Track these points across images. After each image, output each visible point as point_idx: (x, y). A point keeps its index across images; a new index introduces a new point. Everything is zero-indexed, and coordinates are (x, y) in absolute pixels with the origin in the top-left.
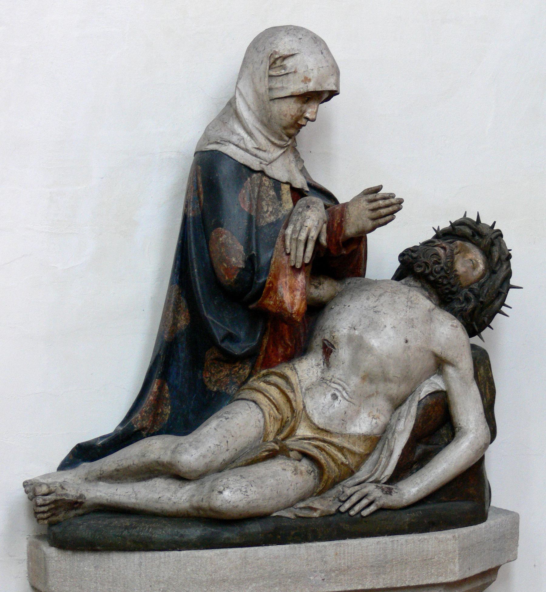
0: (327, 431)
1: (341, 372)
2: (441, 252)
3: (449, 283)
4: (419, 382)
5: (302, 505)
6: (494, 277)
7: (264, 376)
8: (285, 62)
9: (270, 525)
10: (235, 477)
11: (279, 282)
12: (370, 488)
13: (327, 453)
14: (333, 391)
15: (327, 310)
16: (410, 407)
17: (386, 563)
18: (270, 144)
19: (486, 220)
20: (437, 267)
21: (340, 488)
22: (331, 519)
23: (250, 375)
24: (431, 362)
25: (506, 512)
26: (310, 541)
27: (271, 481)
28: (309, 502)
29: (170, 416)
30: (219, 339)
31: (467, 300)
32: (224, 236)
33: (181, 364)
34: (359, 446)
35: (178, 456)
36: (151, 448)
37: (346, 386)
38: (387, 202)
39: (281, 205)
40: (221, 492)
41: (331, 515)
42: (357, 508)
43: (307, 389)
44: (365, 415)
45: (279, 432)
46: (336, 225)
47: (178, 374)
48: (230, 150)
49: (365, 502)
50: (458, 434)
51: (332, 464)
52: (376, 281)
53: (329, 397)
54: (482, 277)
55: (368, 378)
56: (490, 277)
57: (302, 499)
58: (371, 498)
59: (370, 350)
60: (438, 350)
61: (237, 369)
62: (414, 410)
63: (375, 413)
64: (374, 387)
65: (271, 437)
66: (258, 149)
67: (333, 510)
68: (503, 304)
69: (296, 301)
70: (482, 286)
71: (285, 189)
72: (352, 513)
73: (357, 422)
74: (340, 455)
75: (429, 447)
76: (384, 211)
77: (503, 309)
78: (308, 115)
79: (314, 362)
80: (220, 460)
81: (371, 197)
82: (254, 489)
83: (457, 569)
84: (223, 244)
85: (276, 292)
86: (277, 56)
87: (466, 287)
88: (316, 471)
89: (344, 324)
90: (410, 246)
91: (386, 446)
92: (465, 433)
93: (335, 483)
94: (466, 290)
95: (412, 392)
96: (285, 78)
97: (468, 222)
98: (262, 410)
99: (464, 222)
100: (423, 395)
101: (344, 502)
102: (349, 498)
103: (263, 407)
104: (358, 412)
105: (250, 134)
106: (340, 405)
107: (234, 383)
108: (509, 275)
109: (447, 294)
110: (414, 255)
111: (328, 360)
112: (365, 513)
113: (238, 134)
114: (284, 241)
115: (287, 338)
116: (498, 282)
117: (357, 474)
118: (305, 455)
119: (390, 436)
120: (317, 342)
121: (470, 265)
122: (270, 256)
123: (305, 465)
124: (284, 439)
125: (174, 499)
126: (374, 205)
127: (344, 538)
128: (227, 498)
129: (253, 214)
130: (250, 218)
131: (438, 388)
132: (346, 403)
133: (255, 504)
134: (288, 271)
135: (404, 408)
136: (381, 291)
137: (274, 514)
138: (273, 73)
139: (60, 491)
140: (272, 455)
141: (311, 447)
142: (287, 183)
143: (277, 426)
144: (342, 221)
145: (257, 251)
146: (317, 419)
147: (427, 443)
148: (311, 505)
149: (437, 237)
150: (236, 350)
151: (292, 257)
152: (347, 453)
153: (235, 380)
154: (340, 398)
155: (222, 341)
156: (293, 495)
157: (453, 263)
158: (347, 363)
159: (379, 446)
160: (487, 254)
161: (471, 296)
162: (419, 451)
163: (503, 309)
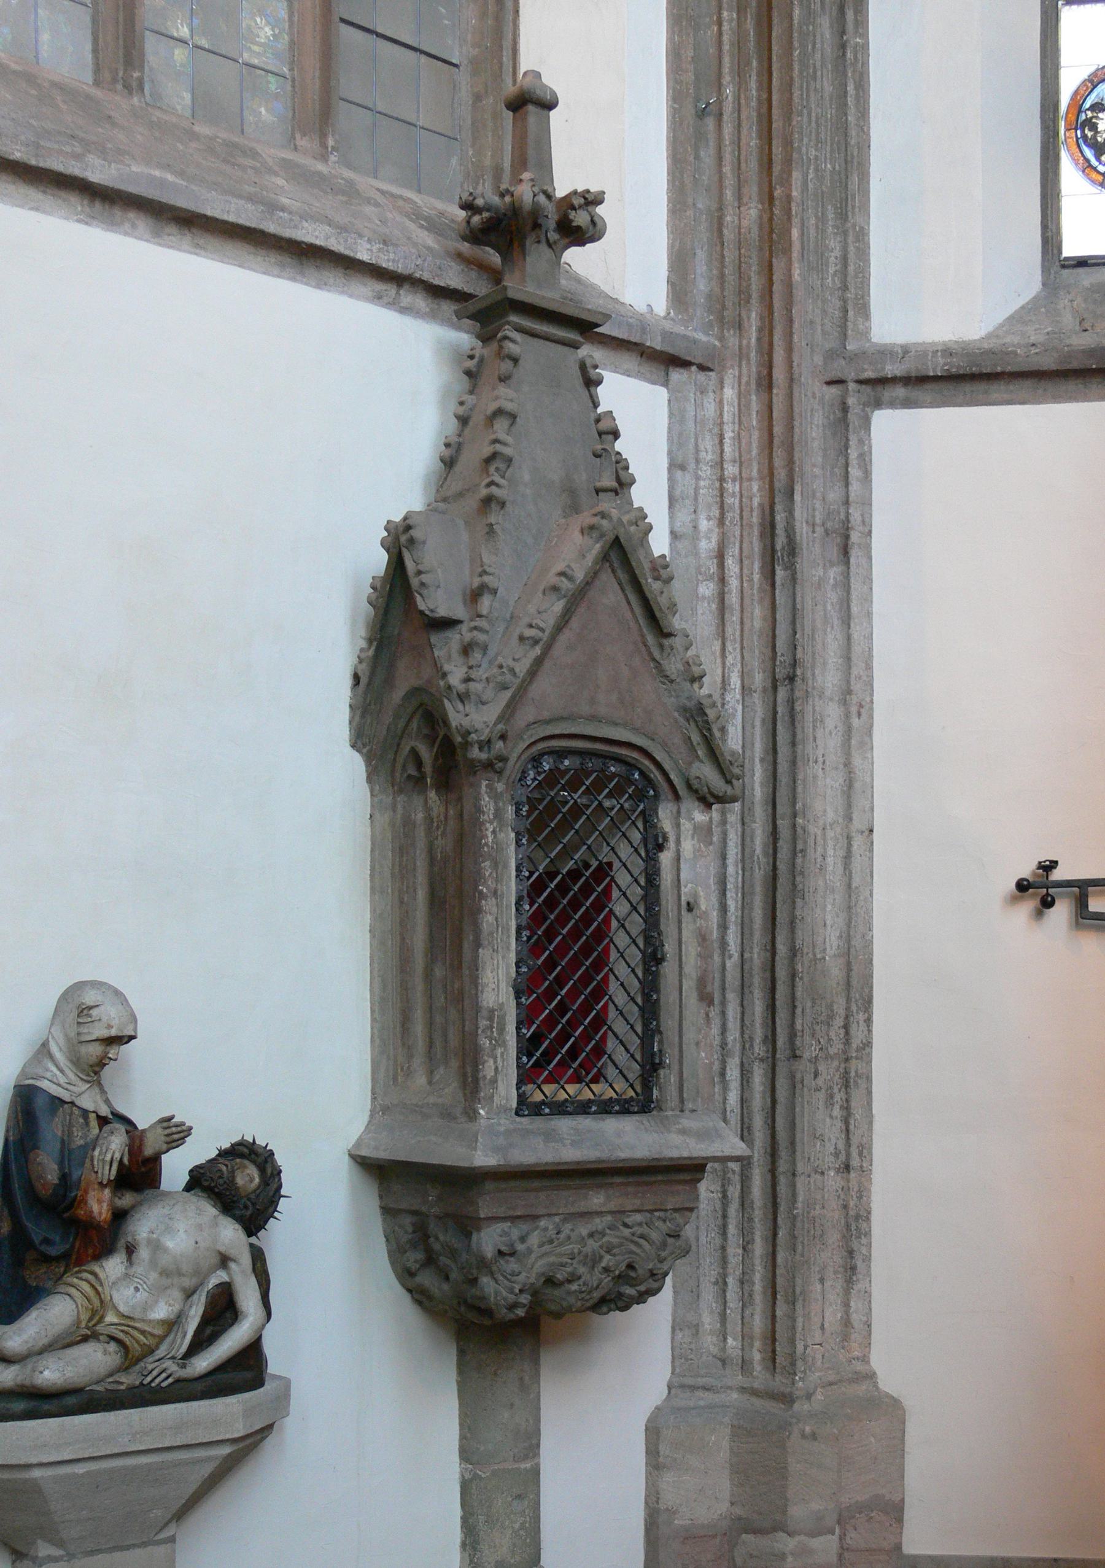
1: (142, 1268)
2: (224, 1168)
3: (231, 1194)
5: (110, 1380)
7: (77, 1272)
12: (168, 1364)
13: (132, 1337)
14: (135, 1285)
15: (128, 1216)
16: (200, 1296)
19: (261, 1142)
20: (221, 1181)
21: (142, 1364)
22: (135, 1390)
24: (216, 1260)
26: (118, 1410)
28: (116, 1378)
31: (246, 1207)
41: (135, 1388)
42: (157, 1381)
44: (163, 1304)
45: (90, 1319)
49: (164, 1375)
51: (136, 1345)
52: (170, 1193)
53: (132, 1289)
54: (258, 1188)
55: (165, 1273)
57: (111, 1375)
58: (169, 1372)
59: (166, 1250)
60: (223, 1249)
62: (203, 1299)
63: (172, 1302)
64: (169, 1281)
65: (83, 1325)
67: (137, 1383)
68: (275, 1210)
70: (258, 1196)
72: (153, 1385)
74: (142, 1337)
77: (276, 1214)
79: (119, 1261)
88: (123, 1351)
90: (198, 1163)
91: (180, 1329)
93: (139, 1360)
95: (202, 1284)
97: (245, 1143)
100: (210, 1286)
101: (146, 1376)
102: (151, 1372)
104: (157, 1302)
106: (142, 1296)
108: (280, 1186)
110: (202, 1171)
112: (164, 1384)
115: (95, 1241)
116: (271, 1193)
119: (184, 1320)
120: (121, 1244)
121: (247, 1179)
123: (113, 1347)
124: (95, 1325)
127: (147, 1406)
131: (223, 1280)
132: (147, 1294)
135: (196, 1297)
136: (175, 1201)
141: (117, 1332)
143: (88, 1314)
146: (122, 1308)
149: (218, 1155)
156: (103, 1371)
157: (234, 1177)
158: (147, 1261)
160: (262, 1169)
161: (249, 1203)
163: (276, 1214)
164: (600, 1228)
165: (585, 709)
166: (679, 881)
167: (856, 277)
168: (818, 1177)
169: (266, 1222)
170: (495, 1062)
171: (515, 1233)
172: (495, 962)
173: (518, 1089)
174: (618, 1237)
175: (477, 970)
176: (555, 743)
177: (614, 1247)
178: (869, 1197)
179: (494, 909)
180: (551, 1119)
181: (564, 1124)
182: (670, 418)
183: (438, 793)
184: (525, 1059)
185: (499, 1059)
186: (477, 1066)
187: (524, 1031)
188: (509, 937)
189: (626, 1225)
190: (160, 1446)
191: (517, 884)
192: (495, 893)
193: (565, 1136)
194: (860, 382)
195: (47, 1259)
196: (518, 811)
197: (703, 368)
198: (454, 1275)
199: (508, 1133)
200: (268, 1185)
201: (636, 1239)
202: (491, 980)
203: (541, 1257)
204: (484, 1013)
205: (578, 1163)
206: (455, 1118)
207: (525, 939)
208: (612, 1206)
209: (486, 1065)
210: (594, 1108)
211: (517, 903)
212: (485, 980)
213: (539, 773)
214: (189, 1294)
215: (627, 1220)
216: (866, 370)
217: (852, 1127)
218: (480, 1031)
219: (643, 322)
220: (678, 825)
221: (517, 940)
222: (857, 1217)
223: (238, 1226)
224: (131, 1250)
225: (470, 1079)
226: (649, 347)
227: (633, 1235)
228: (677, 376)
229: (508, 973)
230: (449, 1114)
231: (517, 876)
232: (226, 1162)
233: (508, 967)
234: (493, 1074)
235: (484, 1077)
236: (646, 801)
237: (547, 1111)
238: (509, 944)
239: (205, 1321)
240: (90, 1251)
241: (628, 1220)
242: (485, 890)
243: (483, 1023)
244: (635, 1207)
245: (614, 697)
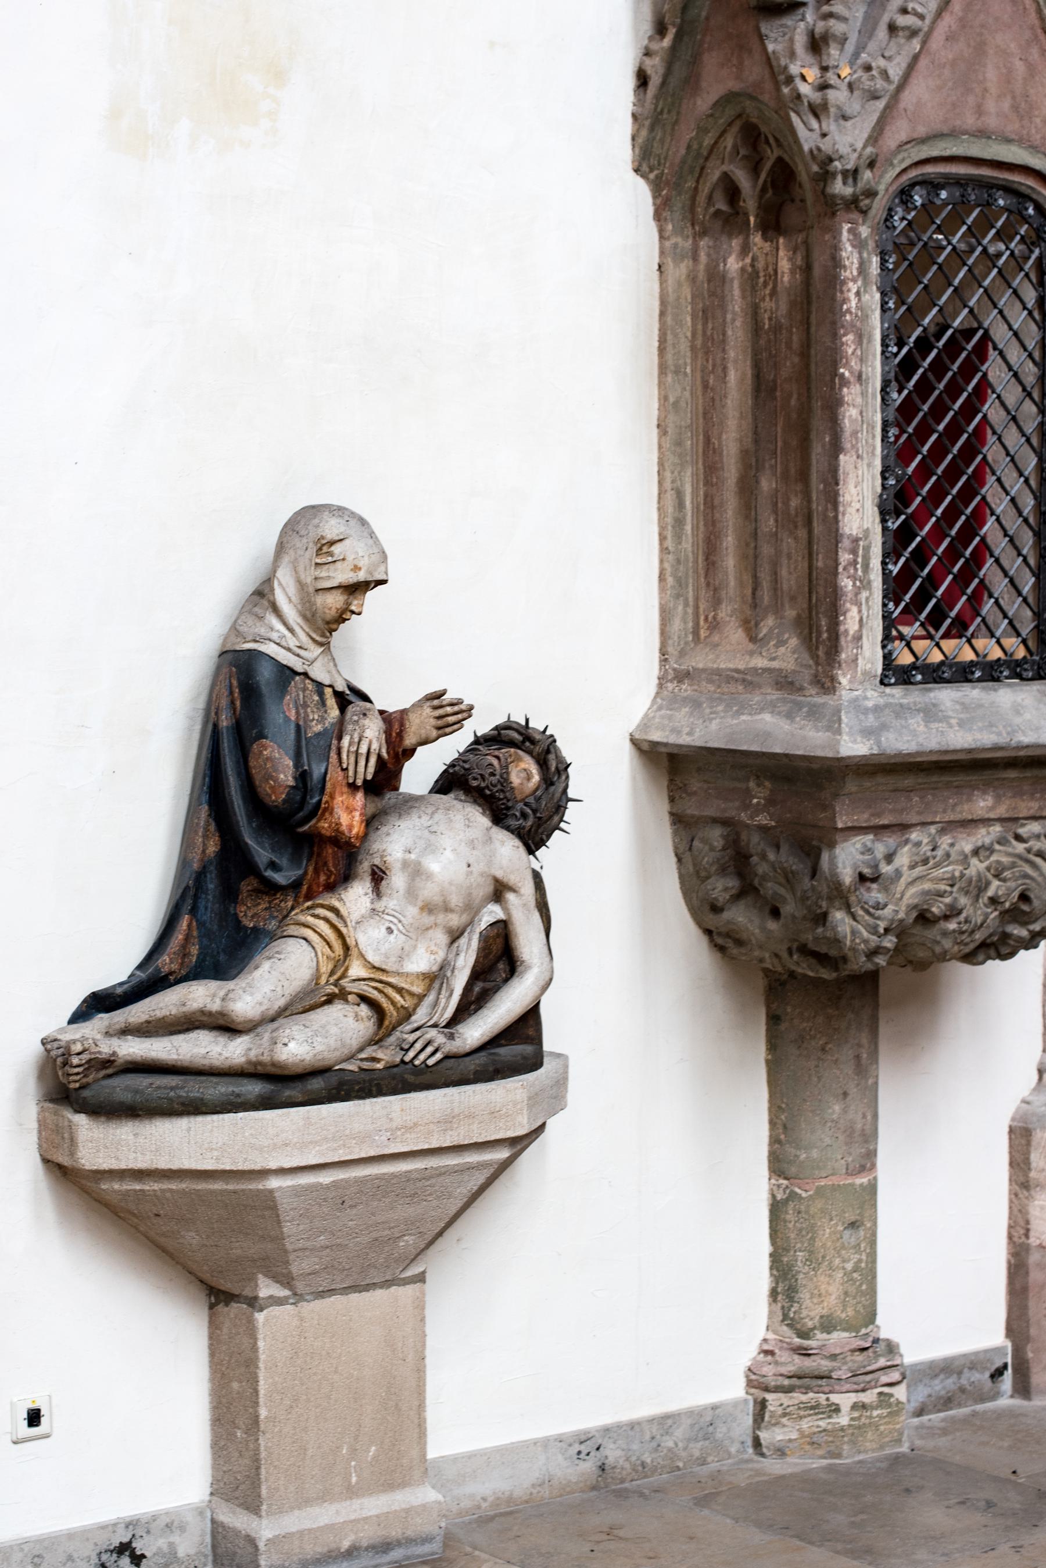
0: (383, 970)
2: (495, 762)
3: (506, 797)
4: (478, 912)
6: (552, 788)
7: (308, 908)
8: (333, 548)
9: (334, 1080)
10: (297, 1027)
11: (335, 802)
12: (432, 1033)
14: (387, 924)
16: (470, 940)
17: (453, 1117)
18: (310, 641)
19: (537, 724)
20: (494, 780)
21: (397, 1034)
22: (395, 1070)
23: (293, 908)
24: (489, 889)
25: (559, 1055)
27: (334, 1030)
29: (198, 958)
30: (262, 867)
31: (524, 816)
32: (270, 749)
33: (210, 897)
34: (418, 986)
35: (232, 1004)
36: (191, 996)
37: (402, 918)
38: (456, 708)
39: (326, 712)
40: (285, 1045)
41: (397, 1066)
42: (422, 1057)
43: (358, 923)
45: (332, 973)
46: (394, 734)
47: (206, 908)
48: (270, 649)
49: (430, 1049)
50: (520, 969)
53: (383, 930)
54: (537, 789)
56: (547, 789)
57: (361, 1049)
58: (436, 1045)
59: (429, 876)
60: (499, 874)
61: (277, 901)
63: (433, 948)
64: (432, 918)
65: (323, 980)
66: (300, 647)
67: (398, 1060)
68: (561, 820)
69: (355, 823)
70: (538, 799)
71: (328, 691)
72: (417, 1062)
73: (414, 958)
75: (488, 985)
76: (451, 719)
77: (562, 825)
78: (353, 608)
80: (276, 1007)
81: (436, 702)
82: (319, 1039)
83: (525, 1121)
84: (268, 759)
85: (331, 813)
86: (324, 542)
87: (521, 801)
89: (396, 847)
92: (529, 967)
94: (520, 805)
95: (471, 923)
96: (331, 566)
98: (313, 948)
99: (508, 726)
100: (483, 925)
101: (407, 1050)
102: (412, 1045)
103: (315, 946)
104: (415, 947)
105: (291, 630)
106: (396, 940)
107: (275, 918)
109: (502, 809)
110: (467, 766)
111: (378, 888)
112: (431, 1062)
113: (278, 631)
114: (339, 753)
116: (558, 795)
117: (413, 1018)
118: (364, 999)
119: (449, 974)
120: (365, 867)
121: (523, 775)
122: (323, 770)
123: (364, 1010)
125: (226, 1054)
126: (441, 712)
127: (409, 1092)
128: (293, 1051)
129: (301, 723)
130: (298, 727)
132: (403, 937)
133: (320, 1057)
134: (345, 789)
135: (463, 941)
137: (337, 1068)
138: (319, 561)
139: (94, 1049)
140: (330, 1000)
141: (371, 990)
142: (330, 686)
143: (330, 966)
144: (401, 731)
145: (309, 765)
146: (371, 957)
147: (485, 981)
148: (374, 1055)
150: (280, 878)
151: (351, 773)
152: (405, 995)
153: (276, 914)
154: (395, 932)
155: (266, 870)
156: (355, 1044)
157: (508, 773)
158: (402, 892)
159: (436, 985)
160: (542, 763)
161: (529, 811)
162: (477, 989)
163: (562, 825)
164: (987, 841)
165: (970, 121)
169: (549, 836)
171: (880, 850)
172: (860, 472)
173: (884, 647)
175: (837, 484)
176: (929, 169)
177: (1004, 869)
179: (859, 400)
180: (930, 690)
181: (946, 696)
183: (765, 238)
185: (864, 607)
186: (837, 617)
188: (874, 437)
189: (1018, 838)
190: (426, 1147)
191: (883, 364)
192: (859, 377)
193: (950, 713)
195: (271, 888)
196: (883, 262)
198: (788, 908)
199: (877, 709)
200: (552, 784)
201: (1031, 857)
202: (855, 499)
203: (912, 883)
204: (846, 543)
205: (970, 751)
206: (801, 689)
207: (892, 439)
208: (1002, 811)
209: (849, 615)
211: (882, 390)
212: (847, 498)
213: (908, 210)
214: (455, 936)
215: (1021, 831)
218: (840, 569)
223: (517, 842)
224: (378, 877)
225: (825, 635)
227: (1029, 851)
229: (873, 487)
230: (792, 683)
231: (883, 353)
232: (496, 753)
233: (873, 478)
234: (856, 627)
235: (846, 631)
237: (919, 677)
238: (874, 448)
239: (477, 974)
240: (322, 878)
241: (1022, 831)
242: (847, 374)
243: (845, 557)
244: (1032, 812)
245: (1006, 105)
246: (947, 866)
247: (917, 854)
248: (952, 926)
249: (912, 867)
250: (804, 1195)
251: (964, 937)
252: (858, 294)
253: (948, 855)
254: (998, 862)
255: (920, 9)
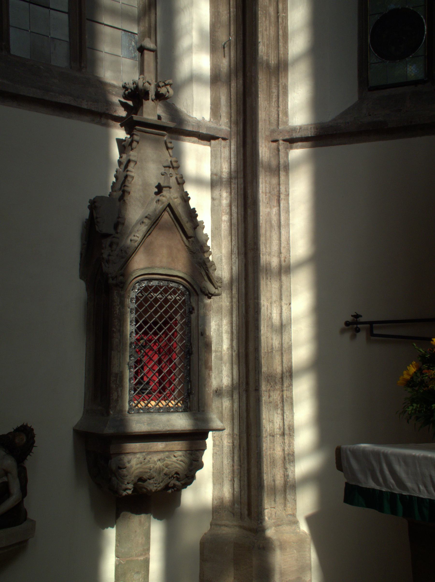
108: (34, 442)
164: (163, 457)
166: (198, 324)
167: (283, 102)
168: (271, 437)
170: (118, 393)
173: (129, 403)
174: (170, 461)
178: (293, 446)
182: (211, 157)
184: (133, 392)
187: (132, 381)
189: (175, 456)
192: (119, 331)
194: (284, 140)
197: (224, 139)
210: (161, 411)
211: (130, 334)
216: (286, 136)
217: (285, 418)
218: (111, 382)
219: (199, 123)
220: (198, 304)
221: (130, 347)
222: (289, 454)
226: (201, 133)
227: (177, 460)
228: (213, 142)
236: (185, 296)
237: (141, 411)
241: (176, 454)
242: (115, 330)
243: (113, 379)
246: (149, 464)
247: (138, 461)
248: (151, 481)
249: (136, 465)
250: (123, 563)
251: (156, 485)
252: (119, 309)
253: (149, 461)
254: (166, 463)
255: (138, 235)
